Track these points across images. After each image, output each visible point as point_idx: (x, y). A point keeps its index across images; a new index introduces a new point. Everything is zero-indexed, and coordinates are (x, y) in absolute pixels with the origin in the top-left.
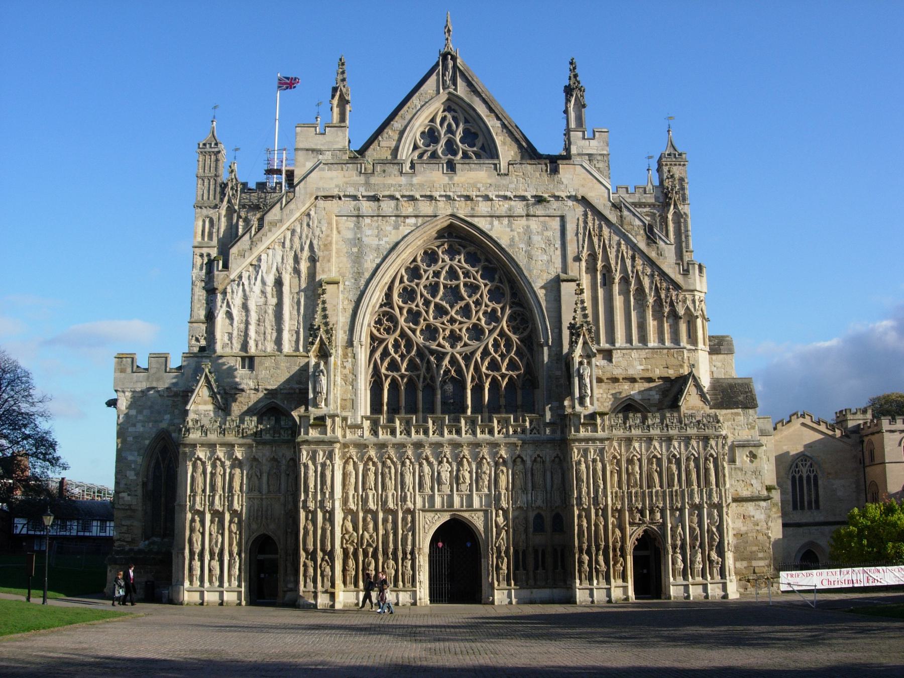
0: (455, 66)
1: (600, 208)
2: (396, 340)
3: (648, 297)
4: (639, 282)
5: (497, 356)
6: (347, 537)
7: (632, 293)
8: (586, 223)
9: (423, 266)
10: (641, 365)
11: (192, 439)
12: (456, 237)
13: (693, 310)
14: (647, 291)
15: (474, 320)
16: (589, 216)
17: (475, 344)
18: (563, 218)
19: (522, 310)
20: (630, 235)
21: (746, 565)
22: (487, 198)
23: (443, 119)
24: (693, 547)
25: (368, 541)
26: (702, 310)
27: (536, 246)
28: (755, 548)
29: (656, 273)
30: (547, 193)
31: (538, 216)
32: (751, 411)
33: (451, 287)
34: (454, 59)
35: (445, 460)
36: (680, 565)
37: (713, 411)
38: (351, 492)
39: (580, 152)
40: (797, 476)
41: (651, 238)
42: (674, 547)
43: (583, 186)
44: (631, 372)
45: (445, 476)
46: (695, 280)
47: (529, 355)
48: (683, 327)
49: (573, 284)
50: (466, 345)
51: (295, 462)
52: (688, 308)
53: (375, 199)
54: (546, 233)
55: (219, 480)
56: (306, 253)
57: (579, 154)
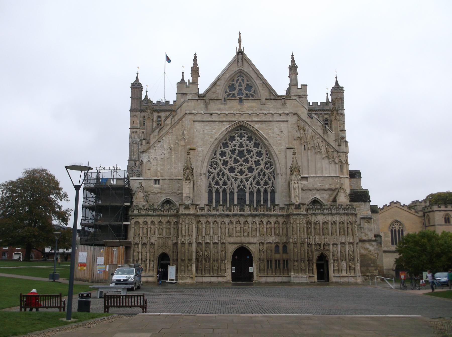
2: (218, 173)
5: (259, 179)
6: (198, 254)
10: (320, 183)
11: (135, 214)
12: (243, 130)
15: (250, 164)
17: (250, 174)
19: (270, 160)
21: (366, 269)
23: (238, 80)
25: (207, 255)
28: (370, 262)
32: (367, 203)
33: (241, 151)
35: (238, 222)
36: (336, 268)
37: (351, 203)
38: (200, 236)
40: (393, 229)
41: (325, 131)
42: (334, 260)
44: (316, 187)
45: (238, 229)
47: (274, 180)
49: (292, 150)
50: (247, 175)
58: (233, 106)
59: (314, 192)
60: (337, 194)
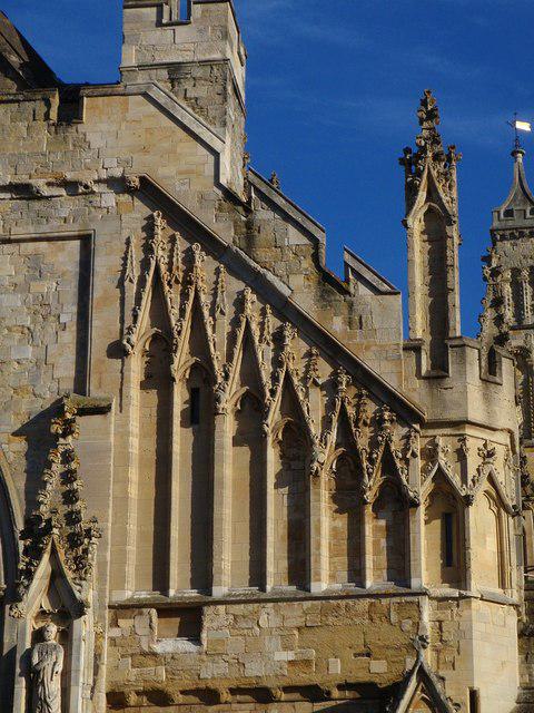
1: (190, 205)
3: (317, 448)
4: (292, 406)
7: (270, 440)
8: (148, 249)
10: (286, 648)
13: (456, 480)
14: (315, 429)
16: (159, 231)
18: (86, 241)
20: (270, 276)
26: (491, 479)
27: (7, 322)
29: (344, 378)
30: (43, 175)
31: (18, 241)
39: (148, 60)
43: (145, 150)
44: (255, 670)
46: (465, 392)
48: (425, 537)
52: (441, 477)
54: (36, 287)
57: (142, 67)
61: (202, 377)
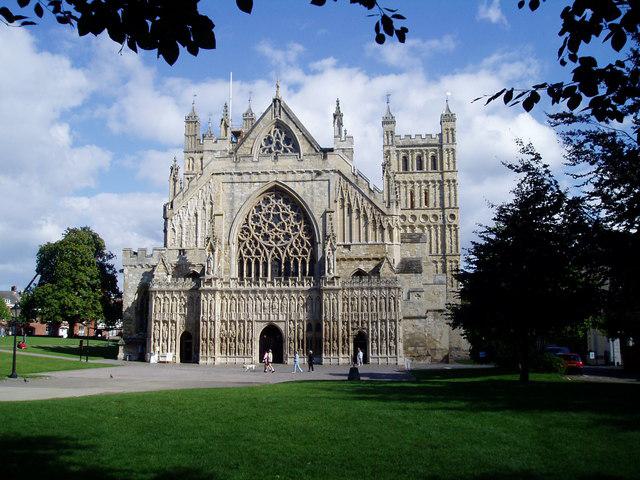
0: (280, 105)
4: (365, 211)
9: (263, 205)
17: (286, 242)
22: (293, 173)
24: (382, 339)
34: (279, 101)
44: (359, 256)
45: (267, 305)
48: (386, 232)
51: (199, 298)
53: (240, 174)
55: (166, 307)
56: (209, 200)
58: (268, 163)
59: (357, 262)
60: (379, 266)
61: (350, 205)
